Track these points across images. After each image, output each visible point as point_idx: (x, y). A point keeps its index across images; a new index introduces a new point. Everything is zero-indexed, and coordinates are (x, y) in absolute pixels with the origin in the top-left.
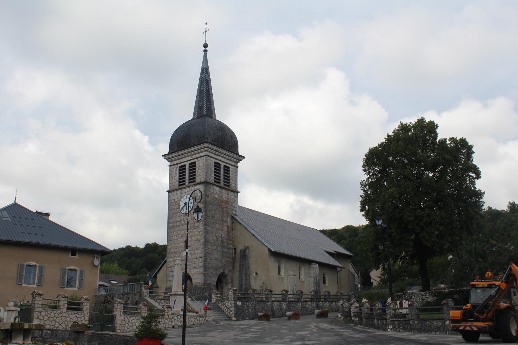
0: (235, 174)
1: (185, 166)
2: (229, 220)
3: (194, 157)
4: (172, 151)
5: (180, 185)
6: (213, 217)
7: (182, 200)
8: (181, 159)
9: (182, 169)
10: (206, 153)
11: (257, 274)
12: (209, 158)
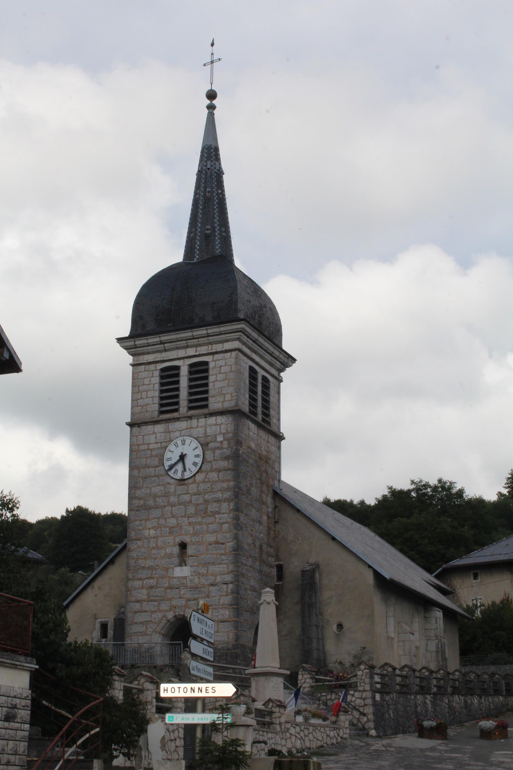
0: (277, 395)
1: (178, 368)
2: (269, 500)
3: (203, 350)
4: (140, 331)
5: (161, 413)
6: (249, 492)
7: (171, 447)
8: (165, 350)
9: (169, 376)
10: (236, 344)
11: (340, 626)
12: (240, 354)
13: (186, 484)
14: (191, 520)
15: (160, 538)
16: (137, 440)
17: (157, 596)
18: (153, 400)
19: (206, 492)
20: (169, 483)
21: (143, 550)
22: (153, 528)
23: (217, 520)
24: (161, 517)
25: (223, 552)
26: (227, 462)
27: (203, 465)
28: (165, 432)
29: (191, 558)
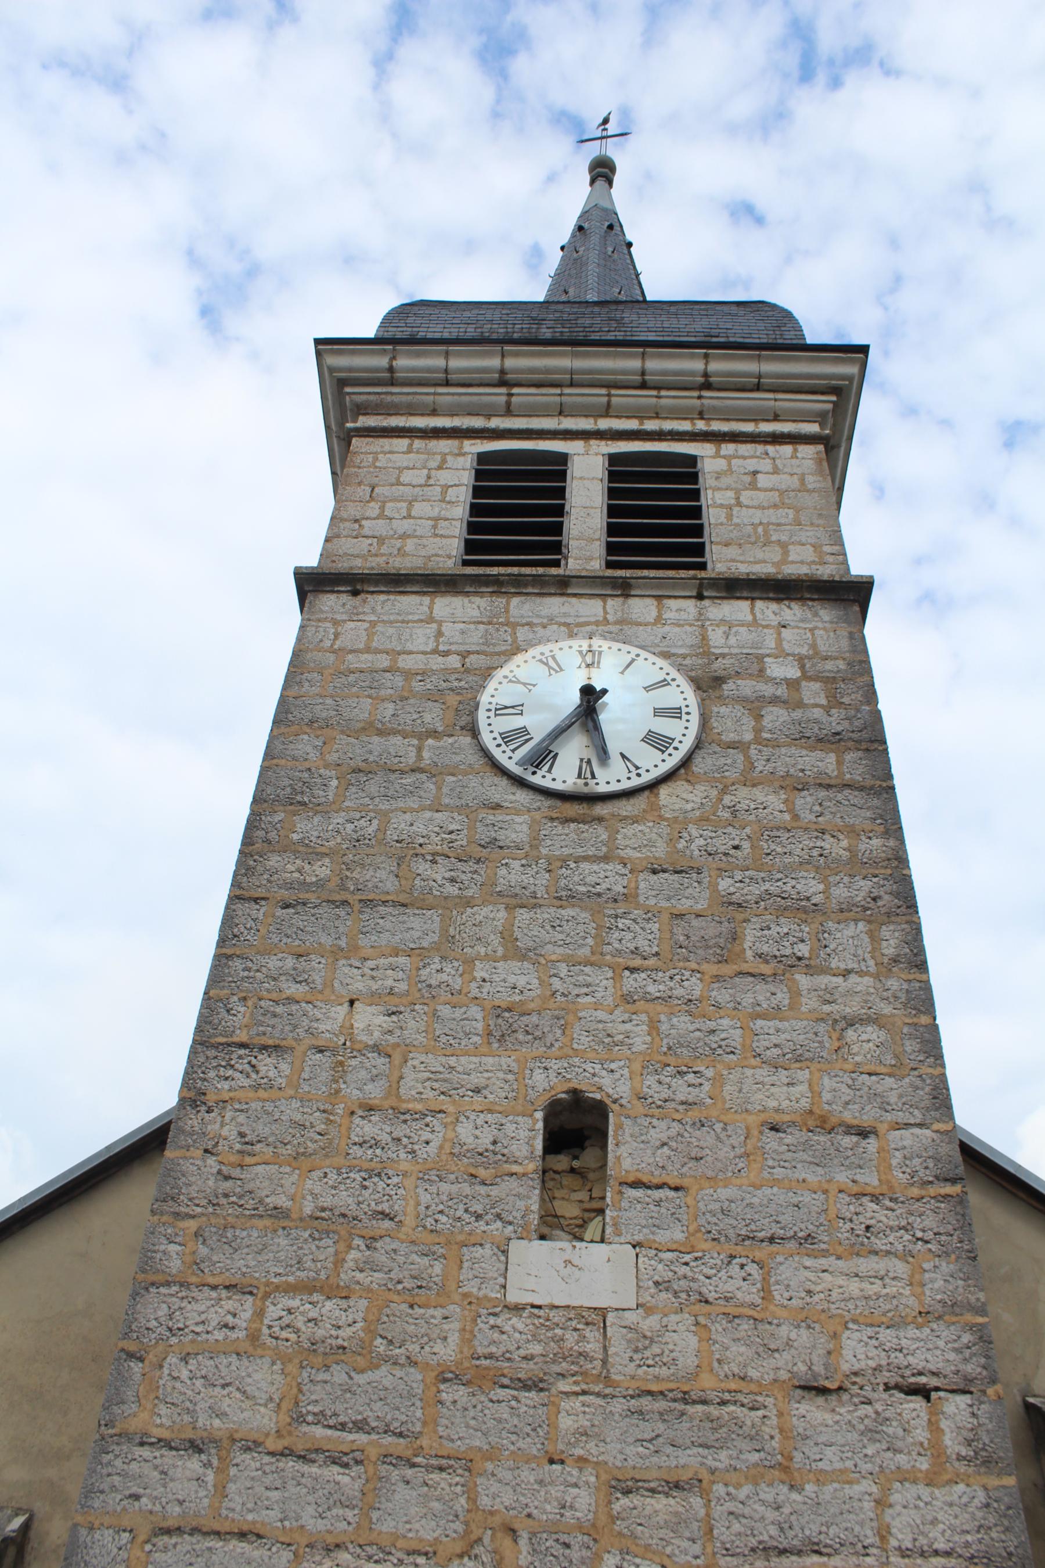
13: (600, 819)
14: (630, 982)
15: (417, 1059)
16: (337, 636)
17: (361, 1426)
18: (435, 527)
19: (724, 862)
20: (498, 806)
21: (291, 1110)
22: (374, 998)
23: (809, 1003)
24: (436, 947)
25: (870, 1179)
26: (832, 758)
27: (701, 753)
28: (490, 623)
29: (638, 1193)
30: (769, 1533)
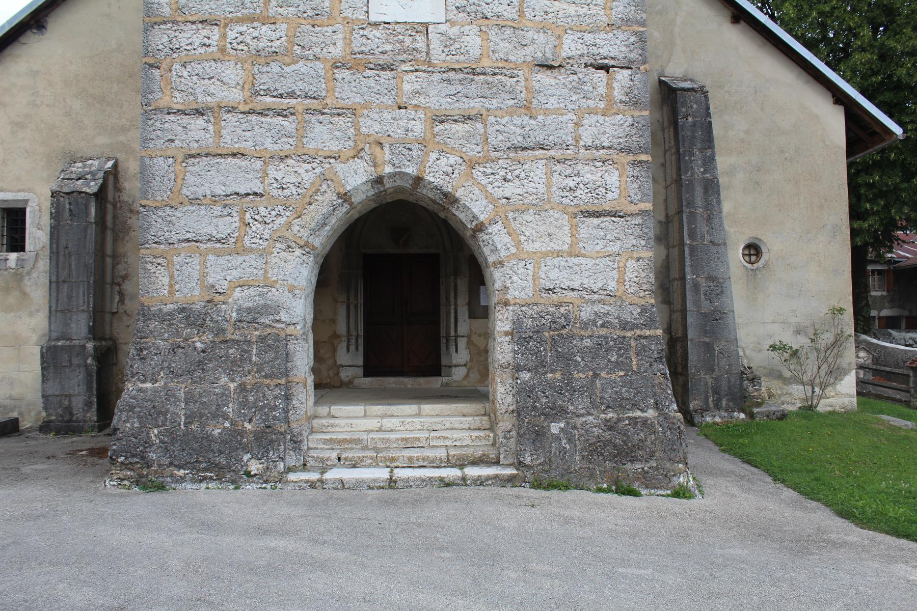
11: (753, 250)
17: (291, 95)
30: (518, 140)
